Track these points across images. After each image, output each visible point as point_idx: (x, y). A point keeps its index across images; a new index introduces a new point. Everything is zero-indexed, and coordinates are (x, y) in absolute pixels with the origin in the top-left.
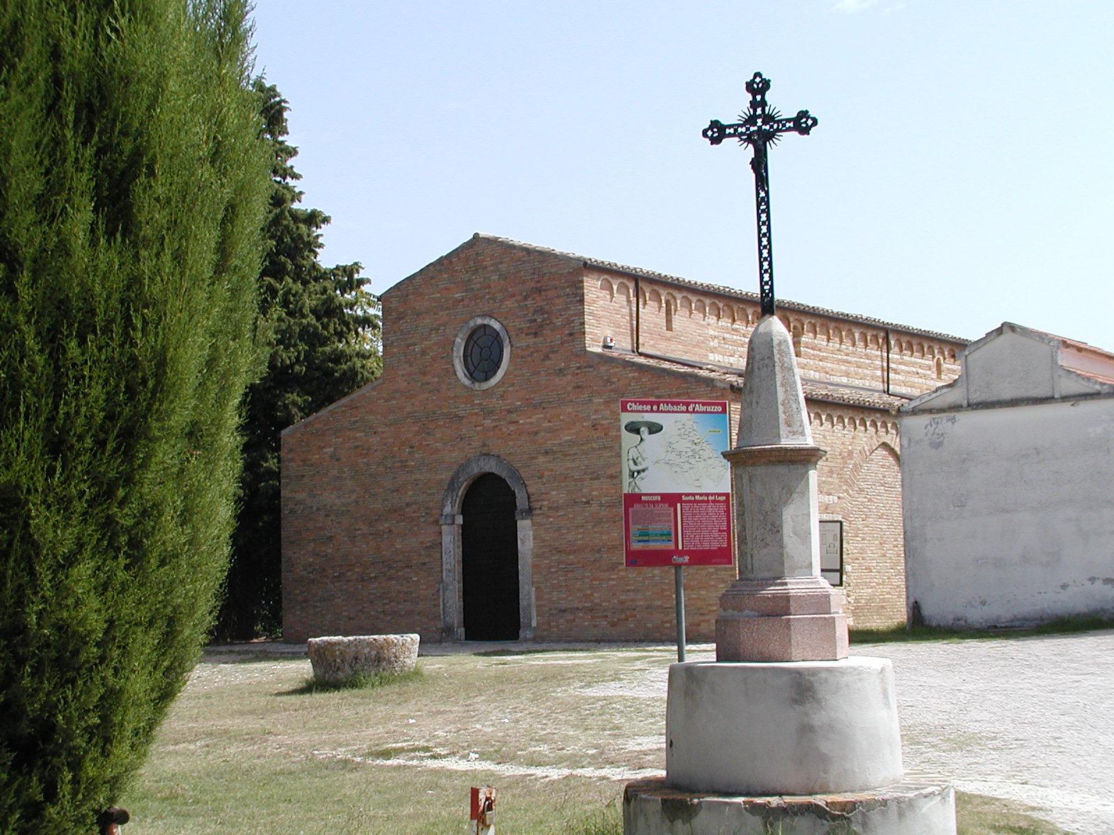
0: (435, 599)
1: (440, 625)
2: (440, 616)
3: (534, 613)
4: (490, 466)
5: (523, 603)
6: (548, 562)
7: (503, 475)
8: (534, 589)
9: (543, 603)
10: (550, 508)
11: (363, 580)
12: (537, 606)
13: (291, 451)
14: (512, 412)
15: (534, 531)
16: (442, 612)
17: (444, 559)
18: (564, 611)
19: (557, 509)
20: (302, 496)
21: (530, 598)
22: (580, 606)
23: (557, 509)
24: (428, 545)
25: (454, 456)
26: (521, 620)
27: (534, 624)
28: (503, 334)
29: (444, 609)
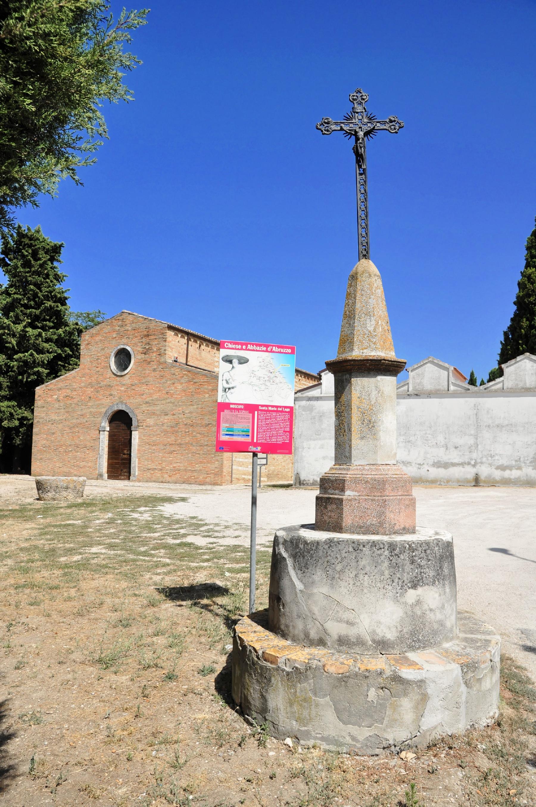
1: (97, 472)
3: (137, 469)
4: (123, 408)
5: (132, 465)
7: (127, 411)
10: (146, 426)
11: (66, 452)
13: (39, 396)
15: (139, 435)
18: (149, 469)
19: (149, 427)
20: (43, 415)
23: (149, 427)
25: (107, 402)
27: (137, 474)
28: (131, 352)
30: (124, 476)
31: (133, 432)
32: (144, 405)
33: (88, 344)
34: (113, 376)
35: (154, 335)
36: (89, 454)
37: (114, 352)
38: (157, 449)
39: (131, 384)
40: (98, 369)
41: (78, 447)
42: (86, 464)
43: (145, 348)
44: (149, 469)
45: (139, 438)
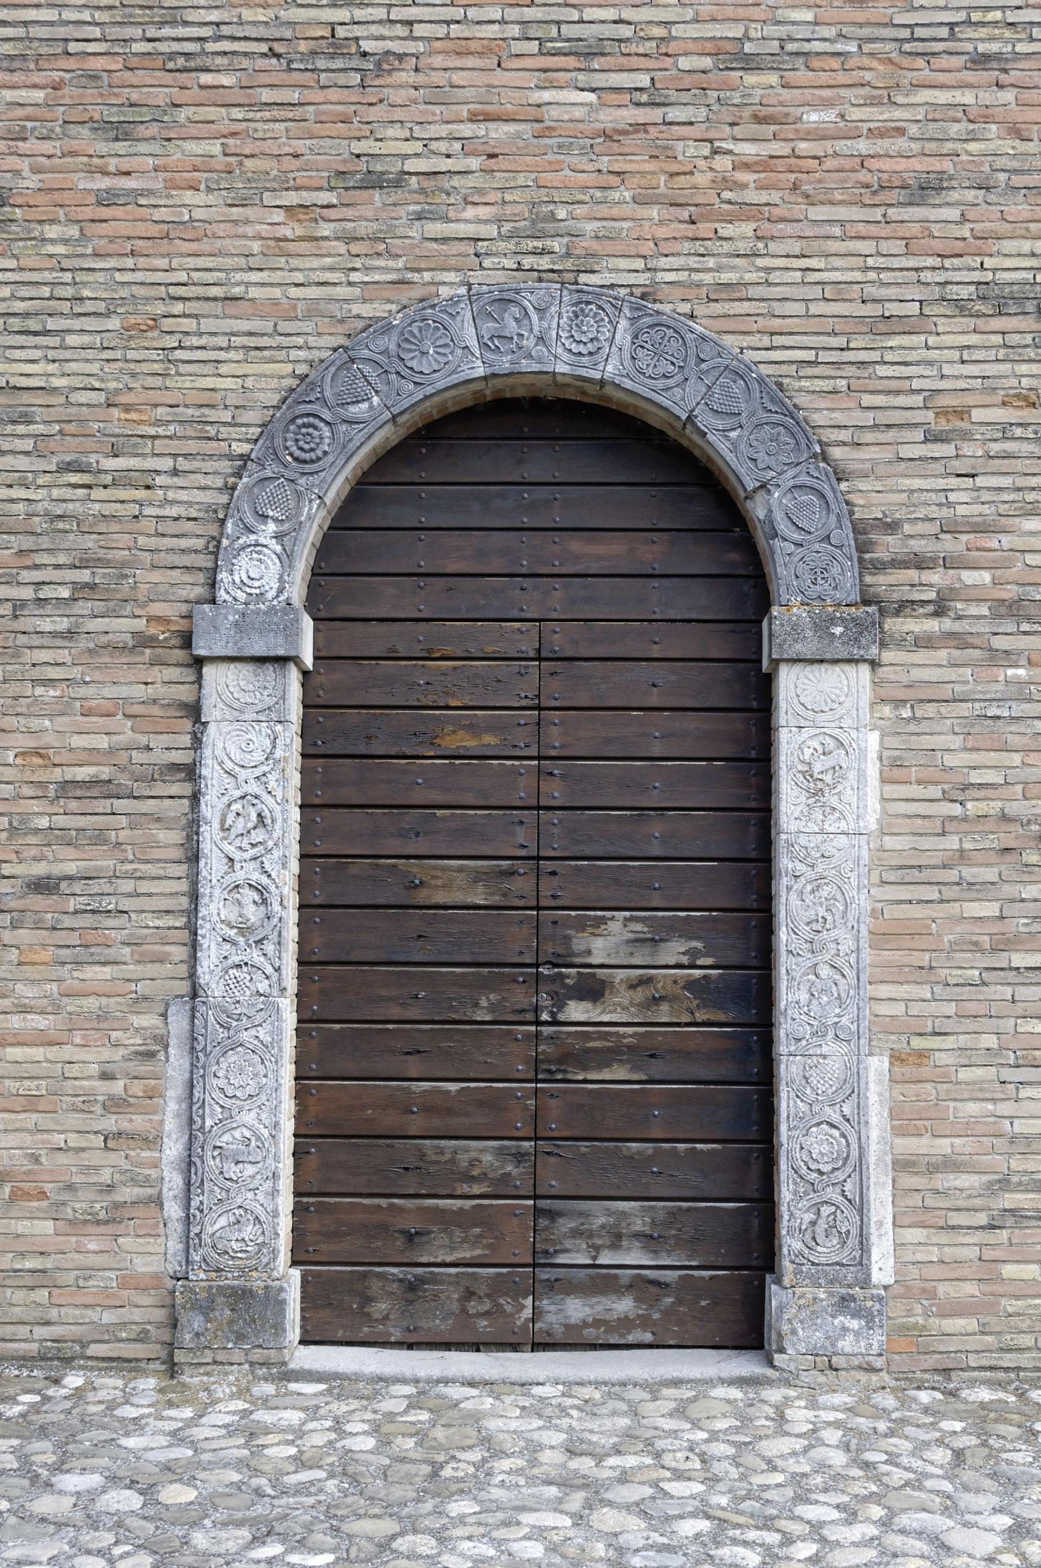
0: (115, 1105)
2: (158, 1202)
6: (992, 909)
8: (878, 1065)
9: (944, 1146)
12: (902, 1165)
14: (750, 63)
16: (173, 1181)
17: (212, 866)
21: (857, 1121)
24: (83, 773)
26: (790, 1244)
29: (189, 1164)
39: (716, 49)
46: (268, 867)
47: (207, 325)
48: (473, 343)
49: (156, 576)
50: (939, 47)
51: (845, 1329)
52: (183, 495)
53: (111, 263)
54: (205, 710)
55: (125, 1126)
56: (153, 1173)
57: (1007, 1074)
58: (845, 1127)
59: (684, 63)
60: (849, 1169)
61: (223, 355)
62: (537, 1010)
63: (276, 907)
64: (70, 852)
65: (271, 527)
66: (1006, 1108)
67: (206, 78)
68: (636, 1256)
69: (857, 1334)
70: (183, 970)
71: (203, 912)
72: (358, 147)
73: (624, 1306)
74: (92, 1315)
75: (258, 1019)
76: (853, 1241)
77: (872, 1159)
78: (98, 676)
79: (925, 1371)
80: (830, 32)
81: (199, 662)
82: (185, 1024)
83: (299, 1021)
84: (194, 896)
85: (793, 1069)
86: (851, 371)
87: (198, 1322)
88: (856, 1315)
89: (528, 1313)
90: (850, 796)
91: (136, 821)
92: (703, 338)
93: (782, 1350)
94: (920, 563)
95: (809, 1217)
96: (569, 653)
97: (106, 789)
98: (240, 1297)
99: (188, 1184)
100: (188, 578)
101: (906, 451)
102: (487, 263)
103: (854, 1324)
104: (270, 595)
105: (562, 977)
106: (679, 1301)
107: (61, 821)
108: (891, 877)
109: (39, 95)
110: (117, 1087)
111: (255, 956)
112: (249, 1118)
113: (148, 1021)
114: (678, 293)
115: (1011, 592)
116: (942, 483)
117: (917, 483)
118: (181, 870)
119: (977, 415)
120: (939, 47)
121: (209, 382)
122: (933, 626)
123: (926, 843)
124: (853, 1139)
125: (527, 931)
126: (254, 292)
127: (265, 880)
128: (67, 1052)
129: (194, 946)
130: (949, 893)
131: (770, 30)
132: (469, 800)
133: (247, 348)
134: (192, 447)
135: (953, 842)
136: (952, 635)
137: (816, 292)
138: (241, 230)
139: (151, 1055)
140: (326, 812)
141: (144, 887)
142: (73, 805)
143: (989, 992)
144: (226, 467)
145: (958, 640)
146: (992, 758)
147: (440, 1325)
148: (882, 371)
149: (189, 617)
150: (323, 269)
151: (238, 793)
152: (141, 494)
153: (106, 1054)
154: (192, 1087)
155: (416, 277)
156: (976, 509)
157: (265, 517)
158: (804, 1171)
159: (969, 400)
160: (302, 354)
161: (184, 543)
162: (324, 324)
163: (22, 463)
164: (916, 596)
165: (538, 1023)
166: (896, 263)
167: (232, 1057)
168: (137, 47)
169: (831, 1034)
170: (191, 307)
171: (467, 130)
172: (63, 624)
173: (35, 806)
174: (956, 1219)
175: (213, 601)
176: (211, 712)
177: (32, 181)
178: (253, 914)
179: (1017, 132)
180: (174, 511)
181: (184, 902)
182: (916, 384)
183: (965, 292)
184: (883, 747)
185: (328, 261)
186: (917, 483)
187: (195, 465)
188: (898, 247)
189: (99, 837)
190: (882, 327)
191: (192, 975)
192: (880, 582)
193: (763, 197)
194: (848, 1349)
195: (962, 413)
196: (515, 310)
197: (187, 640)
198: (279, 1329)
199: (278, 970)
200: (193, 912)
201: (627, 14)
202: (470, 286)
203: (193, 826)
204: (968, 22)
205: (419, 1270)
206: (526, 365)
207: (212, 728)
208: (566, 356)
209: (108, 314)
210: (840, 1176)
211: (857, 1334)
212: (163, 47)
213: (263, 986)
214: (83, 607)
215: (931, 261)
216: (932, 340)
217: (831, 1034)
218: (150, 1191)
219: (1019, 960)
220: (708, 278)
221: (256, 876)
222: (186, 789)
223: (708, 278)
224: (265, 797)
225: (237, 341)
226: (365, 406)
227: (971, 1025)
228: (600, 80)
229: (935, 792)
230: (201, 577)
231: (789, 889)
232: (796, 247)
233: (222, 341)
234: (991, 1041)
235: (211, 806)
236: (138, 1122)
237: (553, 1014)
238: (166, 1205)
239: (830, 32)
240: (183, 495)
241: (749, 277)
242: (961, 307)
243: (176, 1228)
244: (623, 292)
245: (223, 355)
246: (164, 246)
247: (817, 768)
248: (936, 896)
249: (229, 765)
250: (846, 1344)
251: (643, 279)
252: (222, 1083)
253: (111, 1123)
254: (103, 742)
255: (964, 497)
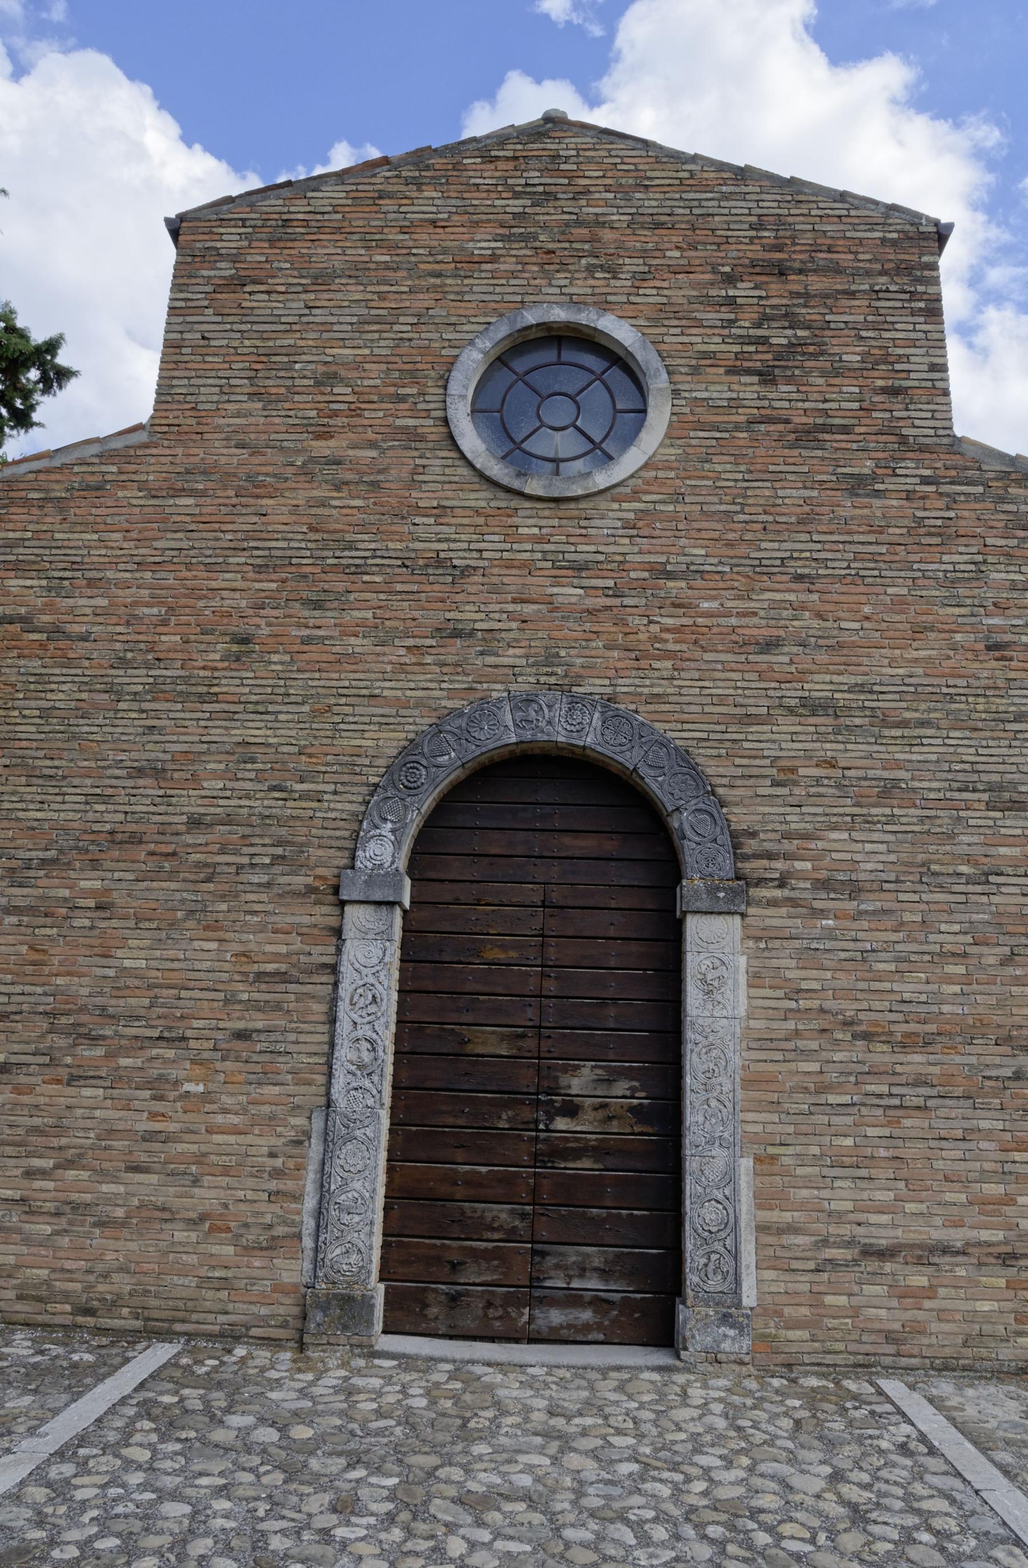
0: (277, 1174)
2: (299, 1237)
6: (815, 1067)
7: (629, 758)
8: (746, 1164)
9: (788, 1217)
10: (824, 885)
12: (762, 1229)
14: (670, 576)
16: (309, 1224)
17: (344, 1026)
18: (885, 1254)
19: (855, 890)
21: (733, 1199)
22: (957, 1237)
23: (855, 890)
24: (270, 967)
26: (692, 1279)
27: (749, 1297)
29: (319, 1213)
30: (573, 1300)
31: (696, 928)
32: (787, 725)
33: (236, 283)
34: (481, 498)
35: (838, 270)
36: (206, 1097)
37: (485, 343)
38: (948, 1079)
40: (323, 448)
41: (94, 1040)
42: (169, 1195)
43: (764, 341)
44: (885, 1254)
45: (755, 979)
46: (377, 1028)
47: (358, 710)
48: (510, 724)
49: (320, 852)
50: (776, 570)
51: (725, 1336)
52: (339, 806)
53: (307, 675)
54: (344, 932)
55: (281, 1187)
56: (297, 1218)
57: (826, 1171)
58: (726, 1203)
59: (633, 575)
60: (728, 1231)
61: (367, 727)
62: (537, 1122)
63: (381, 1053)
64: (260, 1015)
65: (389, 825)
66: (826, 1194)
67: (366, 578)
68: (593, 1283)
69: (733, 1339)
70: (322, 1090)
71: (336, 1054)
72: (448, 616)
73: (586, 1315)
74: (254, 1309)
75: (367, 1122)
76: (730, 1278)
77: (743, 1224)
78: (283, 910)
79: (776, 1365)
80: (715, 561)
81: (342, 904)
82: (322, 1124)
83: (391, 1124)
84: (332, 1045)
85: (694, 1165)
86: (728, 744)
87: (319, 1317)
88: (732, 1326)
89: (526, 1318)
90: (729, 994)
91: (300, 997)
92: (643, 724)
93: (686, 1349)
94: (770, 856)
95: (703, 1261)
96: (561, 903)
97: (283, 977)
98: (346, 1301)
99: (318, 1226)
100: (339, 854)
101: (761, 791)
102: (520, 679)
103: (732, 1332)
104: (386, 865)
105: (552, 1101)
106: (621, 1314)
107: (255, 996)
108: (754, 1045)
109: (274, 586)
110: (278, 1162)
111: (367, 1083)
112: (357, 1185)
113: (299, 1121)
114: (630, 698)
115: (823, 875)
116: (782, 810)
117: (767, 810)
118: (325, 1028)
119: (802, 771)
120: (776, 570)
121: (358, 742)
122: (778, 893)
123: (775, 1025)
124: (731, 1211)
125: (532, 1071)
126: (386, 693)
127: (375, 1036)
128: (249, 1139)
129: (330, 1075)
130: (790, 1056)
131: (681, 559)
132: (500, 990)
133: (381, 724)
134: (346, 778)
135: (791, 1025)
136: (789, 899)
137: (708, 700)
138: (381, 659)
139: (300, 1143)
140: (413, 995)
141: (303, 1038)
142: (263, 987)
143: (814, 1119)
144: (364, 790)
145: (793, 902)
146: (814, 973)
147: (469, 1323)
148: (746, 745)
149: (338, 876)
150: (426, 681)
151: (361, 983)
152: (315, 805)
153: (273, 1141)
154: (324, 1164)
155: (479, 686)
156: (802, 825)
157: (385, 820)
158: (700, 1231)
159: (797, 763)
160: (412, 727)
161: (338, 833)
162: (425, 711)
163: (248, 785)
164: (768, 876)
165: (537, 1130)
166: (753, 685)
167: (349, 1146)
168: (329, 561)
169: (717, 1143)
170: (350, 700)
171: (511, 607)
172: (265, 879)
173: (241, 987)
174: (795, 1265)
175: (353, 868)
176: (349, 933)
177: (266, 631)
178: (367, 1057)
179: (820, 616)
180: (333, 815)
181: (326, 1048)
182: (766, 753)
183: (793, 702)
184: (749, 965)
185: (429, 676)
186: (767, 810)
187: (347, 788)
188: (754, 676)
189: (278, 1007)
190: (746, 720)
191: (328, 1094)
192: (747, 866)
193: (678, 647)
194: (727, 1349)
195: (793, 770)
196: (535, 706)
197: (336, 890)
198: (370, 1323)
199: (380, 1092)
200: (330, 1055)
201: (601, 549)
202: (509, 692)
203: (333, 1001)
204: (791, 558)
205: (459, 1288)
206: (541, 737)
207: (348, 943)
208: (564, 732)
209: (303, 703)
210: (723, 1235)
211: (733, 1339)
212: (344, 561)
213: (370, 1102)
214: (277, 869)
215: (773, 685)
216: (775, 729)
217: (717, 1143)
218: (294, 1230)
219: (832, 1099)
220: (646, 690)
221: (370, 1034)
222: (330, 979)
223: (646, 690)
224: (377, 985)
225: (375, 719)
226: (446, 757)
227: (803, 1139)
228: (586, 583)
229: (780, 993)
230: (347, 854)
231: (692, 1051)
232: (696, 675)
233: (367, 720)
234: (815, 1150)
235: (345, 990)
236: (290, 1185)
237: (546, 1125)
238: (304, 1239)
239: (715, 561)
240: (339, 806)
241: (669, 691)
242: (791, 711)
243: (309, 1254)
244: (597, 697)
245: (367, 727)
246: (337, 666)
247: (709, 977)
248: (781, 1058)
249: (357, 965)
250: (726, 1346)
251: (609, 690)
252: (342, 1162)
253: (273, 1185)
254: (283, 949)
255: (795, 818)
